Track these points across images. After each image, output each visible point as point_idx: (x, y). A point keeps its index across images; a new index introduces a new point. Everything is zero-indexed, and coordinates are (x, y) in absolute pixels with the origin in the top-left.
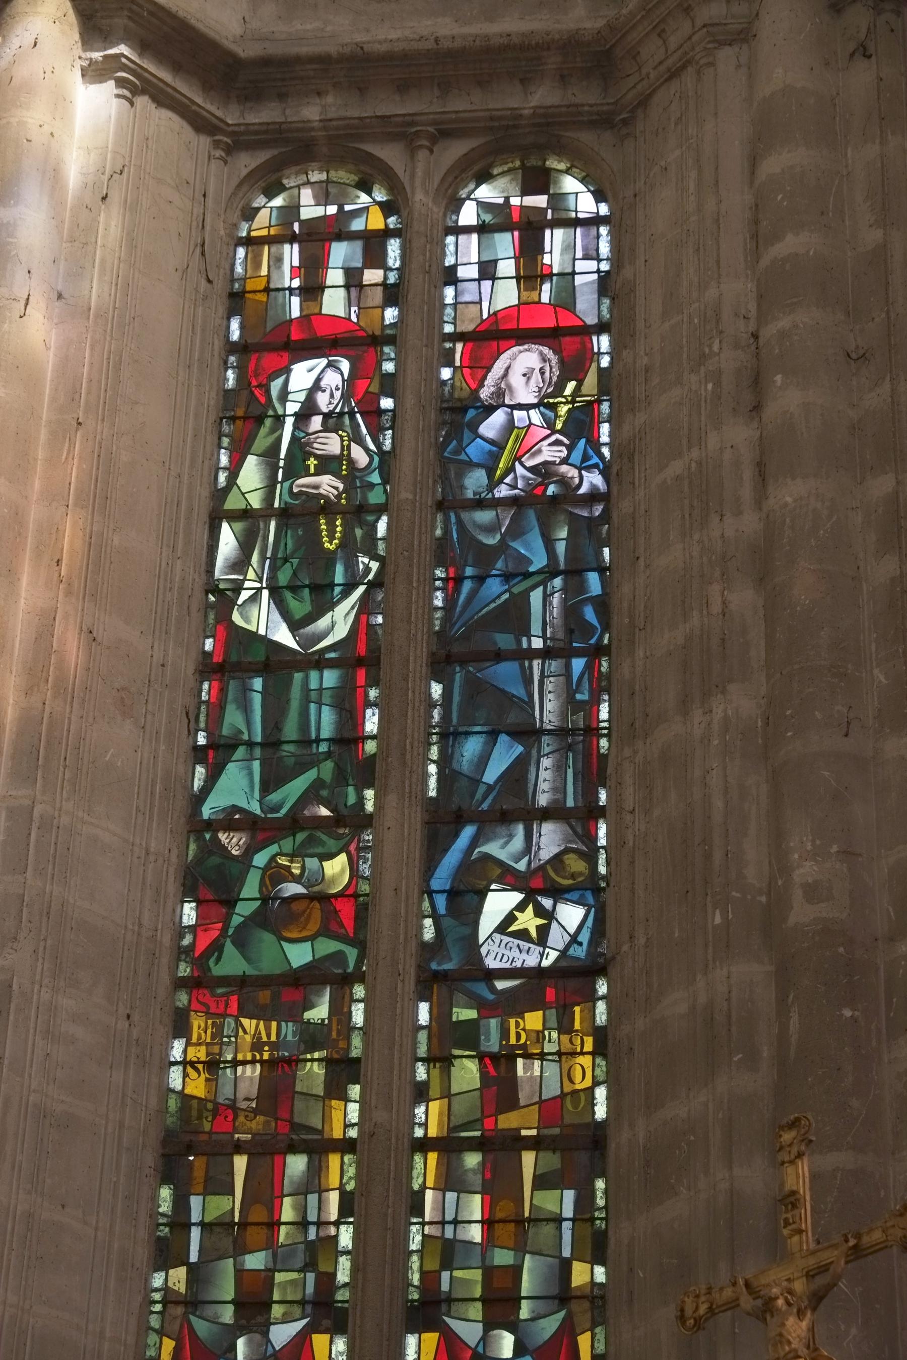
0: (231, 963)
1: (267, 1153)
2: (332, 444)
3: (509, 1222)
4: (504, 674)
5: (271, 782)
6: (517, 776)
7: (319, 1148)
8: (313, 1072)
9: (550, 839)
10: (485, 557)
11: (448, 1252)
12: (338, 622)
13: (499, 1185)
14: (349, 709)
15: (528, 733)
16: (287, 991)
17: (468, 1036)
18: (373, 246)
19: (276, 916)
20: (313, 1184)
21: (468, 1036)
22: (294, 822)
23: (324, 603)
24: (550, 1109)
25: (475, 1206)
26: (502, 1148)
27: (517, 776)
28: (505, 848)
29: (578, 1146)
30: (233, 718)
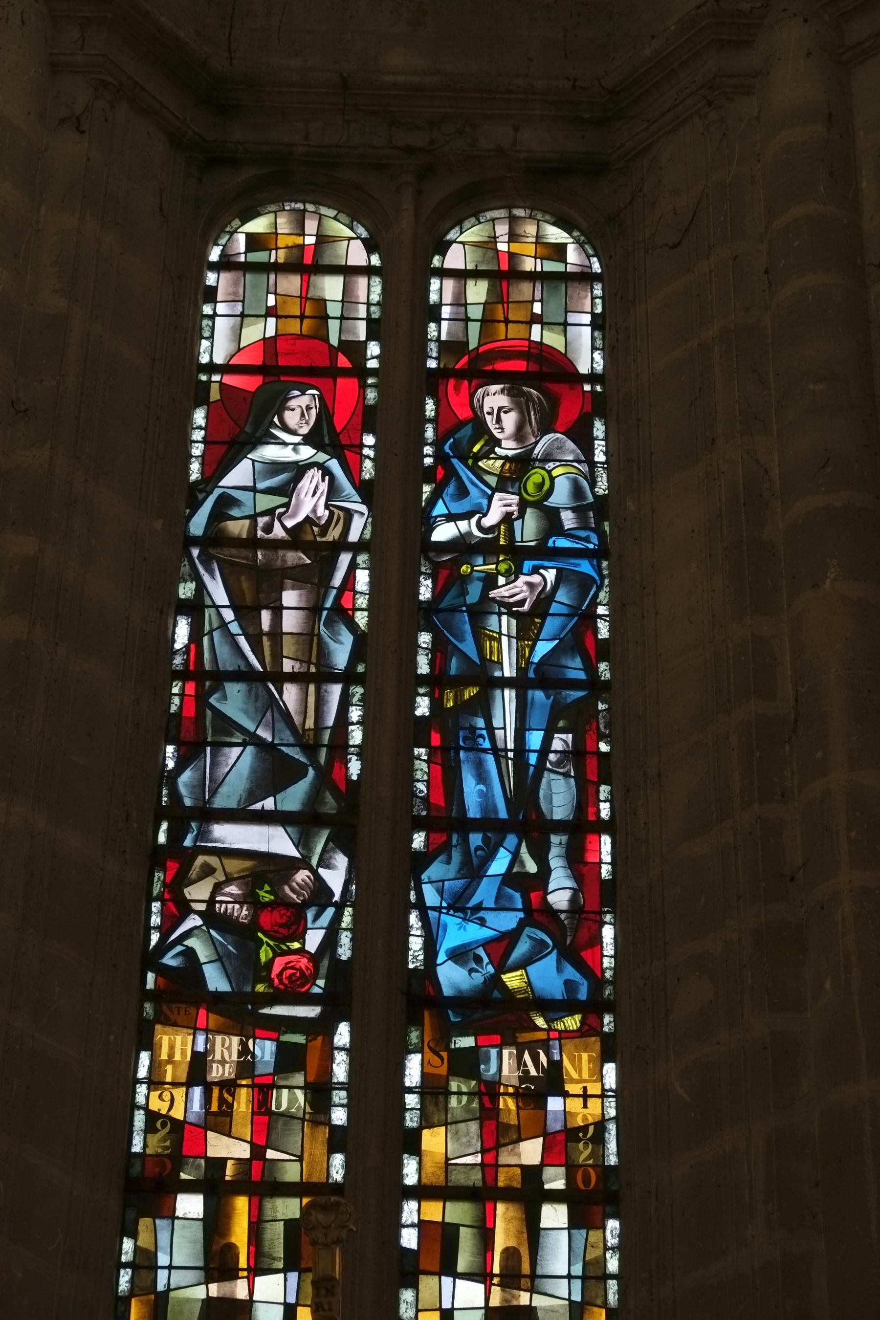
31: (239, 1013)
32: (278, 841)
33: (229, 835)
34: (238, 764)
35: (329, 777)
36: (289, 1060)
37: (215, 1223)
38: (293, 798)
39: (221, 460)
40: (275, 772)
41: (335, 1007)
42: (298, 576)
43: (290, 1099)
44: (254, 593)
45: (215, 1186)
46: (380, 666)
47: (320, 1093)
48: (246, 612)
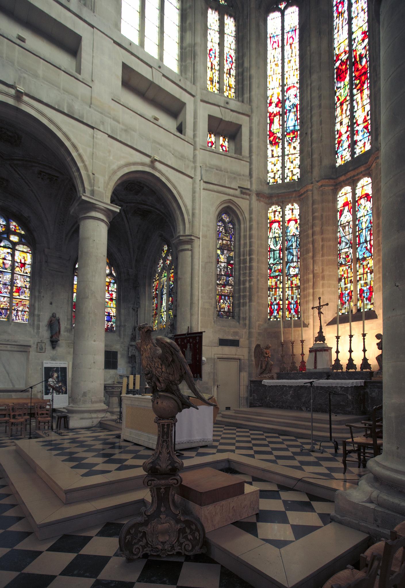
0: (272, 275)
1: (276, 289)
2: (277, 231)
3: (293, 293)
4: (291, 251)
5: (274, 260)
6: (292, 259)
7: (279, 288)
8: (278, 282)
9: (295, 264)
10: (289, 241)
11: (289, 295)
12: (278, 247)
13: (292, 290)
14: (280, 254)
15: (293, 255)
16: (276, 277)
17: (289, 279)
18: (279, 212)
19: (275, 271)
20: (279, 291)
21: (289, 279)
22: (276, 263)
23: (277, 245)
24: (296, 285)
25: (290, 292)
26: (292, 288)
27: (292, 259)
28: (292, 265)
29: (298, 287)
30: (271, 255)
31: (345, 265)
32: (347, 250)
33: (343, 251)
34: (344, 244)
35: (351, 243)
36: (349, 267)
37: (345, 281)
38: (348, 246)
39: (340, 218)
40: (347, 244)
41: (352, 262)
42: (347, 225)
43: (349, 270)
44: (344, 227)
45: (345, 278)
46: (354, 232)
47: (351, 269)
48: (343, 230)
